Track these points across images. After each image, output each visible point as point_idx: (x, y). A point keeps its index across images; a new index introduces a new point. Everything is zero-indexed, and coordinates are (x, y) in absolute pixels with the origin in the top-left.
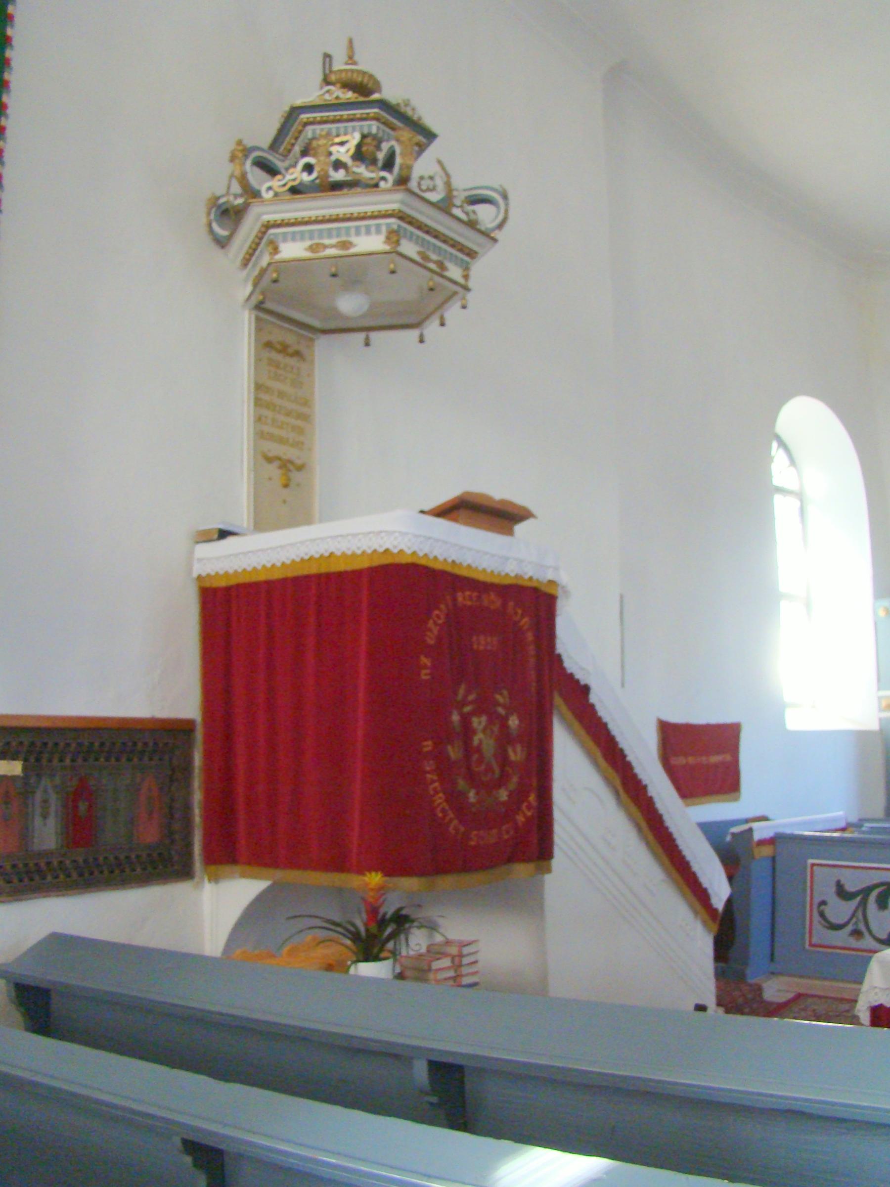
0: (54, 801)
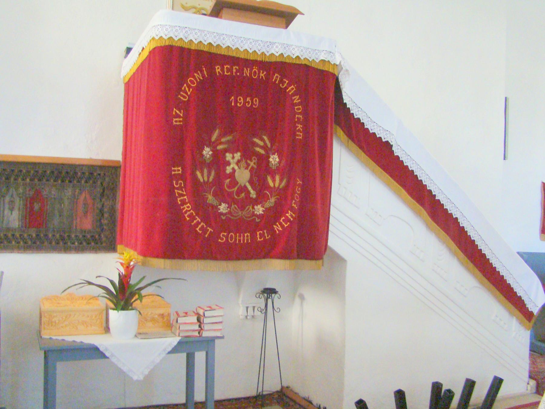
0: (18, 203)
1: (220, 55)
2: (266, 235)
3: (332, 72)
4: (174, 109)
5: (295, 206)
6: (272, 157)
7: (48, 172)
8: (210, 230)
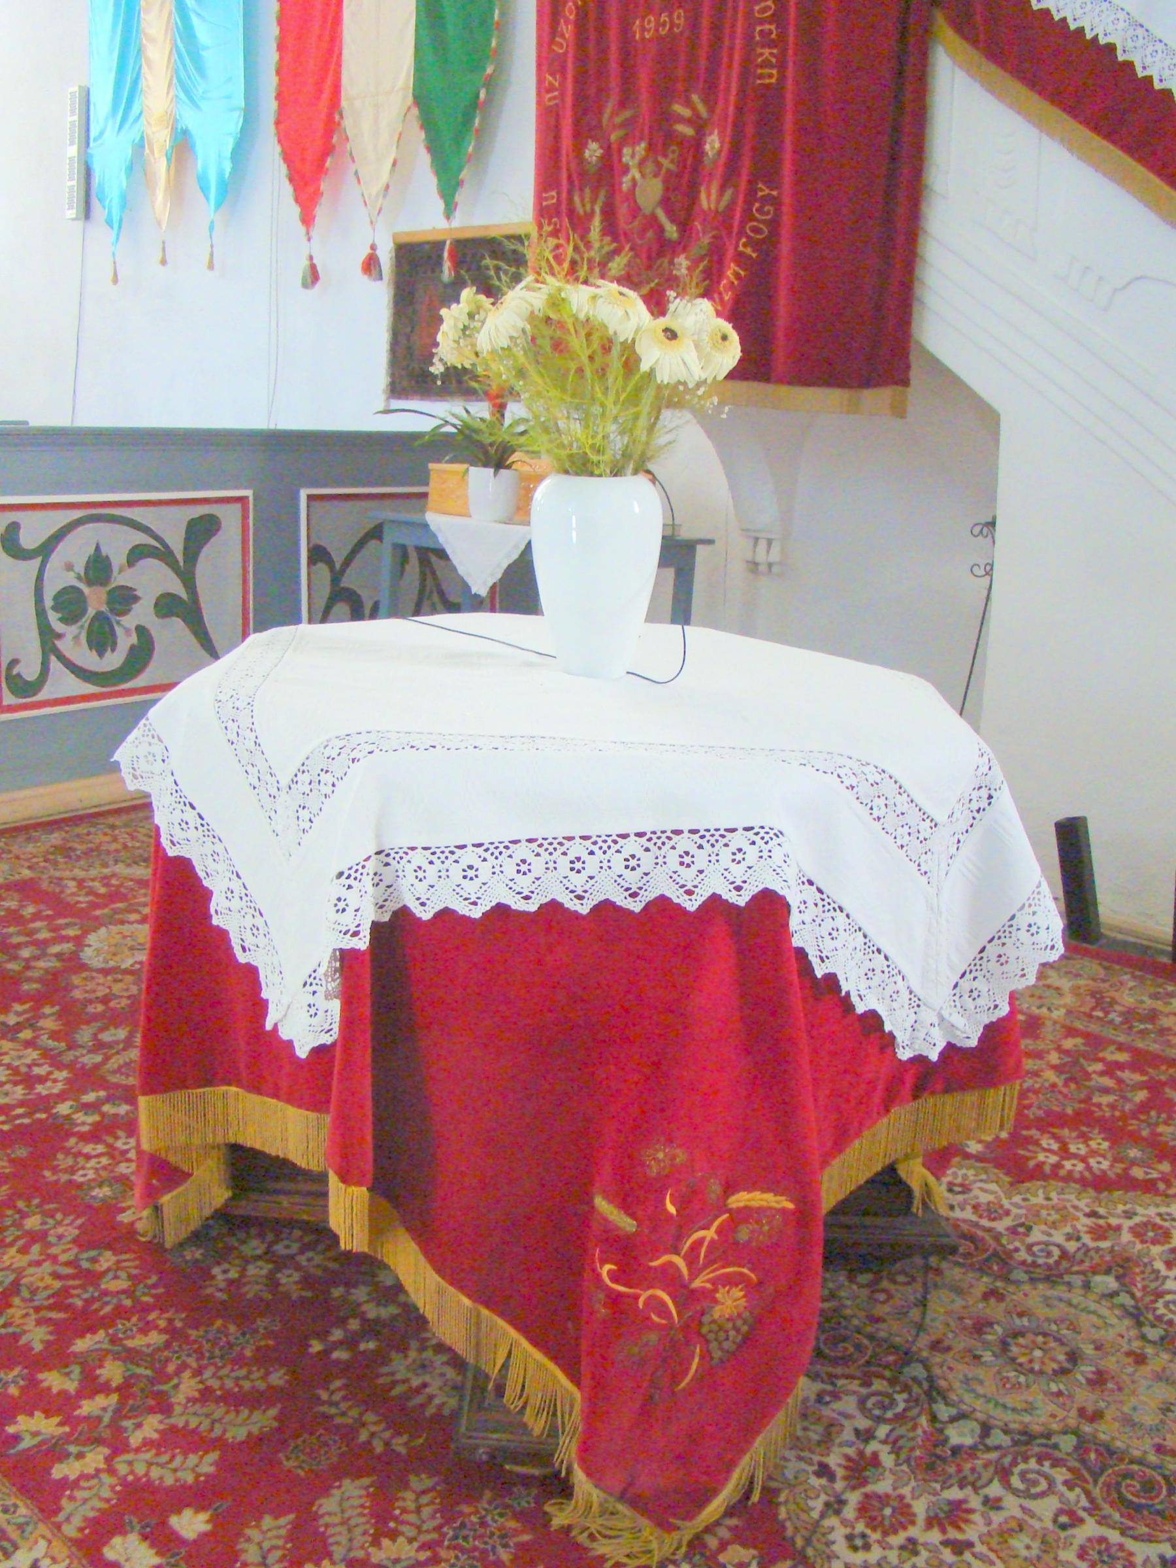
5: (749, 251)
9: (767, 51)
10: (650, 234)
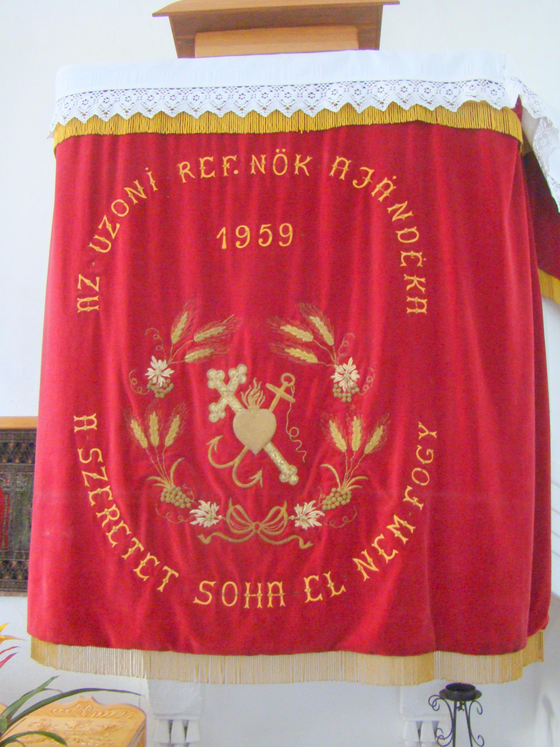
1: (190, 135)
2: (331, 585)
3: (500, 130)
4: (80, 277)
5: (415, 501)
6: (339, 369)
7: (11, 445)
8: (171, 572)
9: (415, 279)
10: (258, 477)
